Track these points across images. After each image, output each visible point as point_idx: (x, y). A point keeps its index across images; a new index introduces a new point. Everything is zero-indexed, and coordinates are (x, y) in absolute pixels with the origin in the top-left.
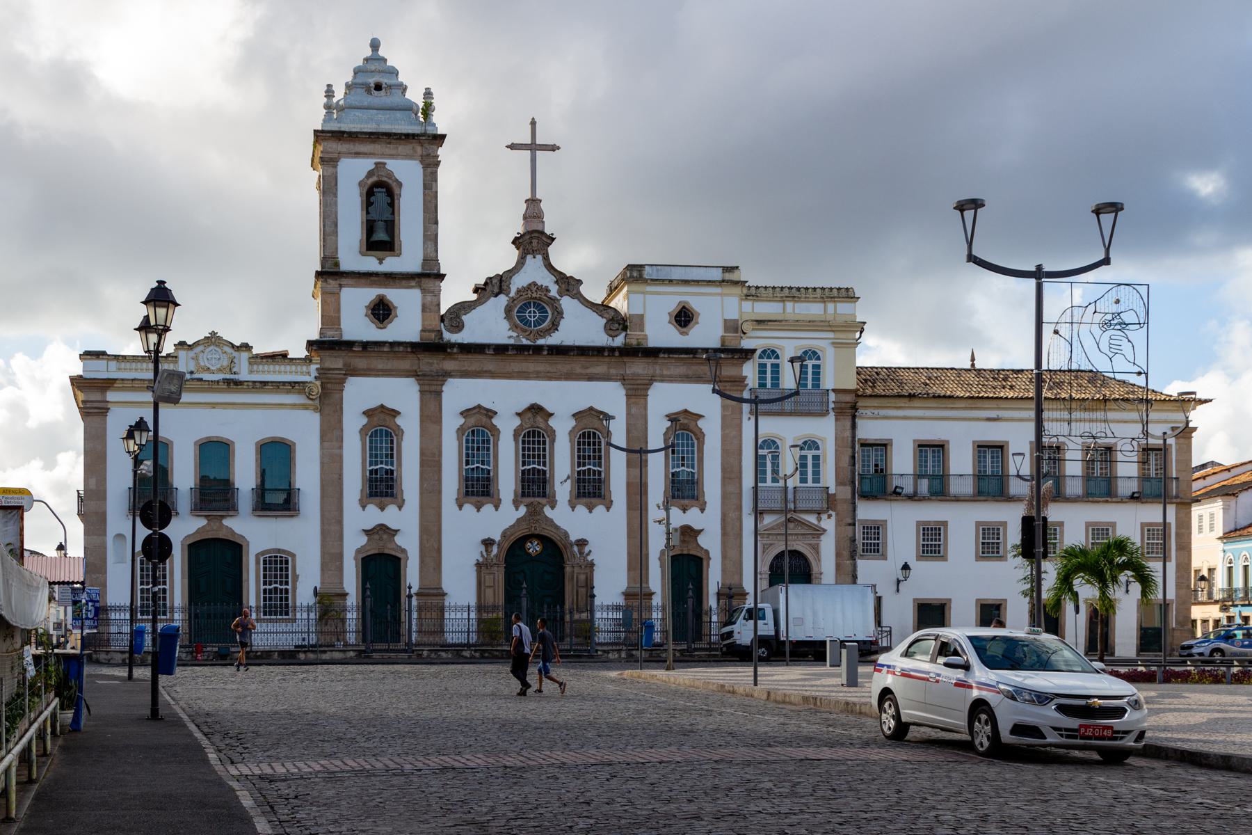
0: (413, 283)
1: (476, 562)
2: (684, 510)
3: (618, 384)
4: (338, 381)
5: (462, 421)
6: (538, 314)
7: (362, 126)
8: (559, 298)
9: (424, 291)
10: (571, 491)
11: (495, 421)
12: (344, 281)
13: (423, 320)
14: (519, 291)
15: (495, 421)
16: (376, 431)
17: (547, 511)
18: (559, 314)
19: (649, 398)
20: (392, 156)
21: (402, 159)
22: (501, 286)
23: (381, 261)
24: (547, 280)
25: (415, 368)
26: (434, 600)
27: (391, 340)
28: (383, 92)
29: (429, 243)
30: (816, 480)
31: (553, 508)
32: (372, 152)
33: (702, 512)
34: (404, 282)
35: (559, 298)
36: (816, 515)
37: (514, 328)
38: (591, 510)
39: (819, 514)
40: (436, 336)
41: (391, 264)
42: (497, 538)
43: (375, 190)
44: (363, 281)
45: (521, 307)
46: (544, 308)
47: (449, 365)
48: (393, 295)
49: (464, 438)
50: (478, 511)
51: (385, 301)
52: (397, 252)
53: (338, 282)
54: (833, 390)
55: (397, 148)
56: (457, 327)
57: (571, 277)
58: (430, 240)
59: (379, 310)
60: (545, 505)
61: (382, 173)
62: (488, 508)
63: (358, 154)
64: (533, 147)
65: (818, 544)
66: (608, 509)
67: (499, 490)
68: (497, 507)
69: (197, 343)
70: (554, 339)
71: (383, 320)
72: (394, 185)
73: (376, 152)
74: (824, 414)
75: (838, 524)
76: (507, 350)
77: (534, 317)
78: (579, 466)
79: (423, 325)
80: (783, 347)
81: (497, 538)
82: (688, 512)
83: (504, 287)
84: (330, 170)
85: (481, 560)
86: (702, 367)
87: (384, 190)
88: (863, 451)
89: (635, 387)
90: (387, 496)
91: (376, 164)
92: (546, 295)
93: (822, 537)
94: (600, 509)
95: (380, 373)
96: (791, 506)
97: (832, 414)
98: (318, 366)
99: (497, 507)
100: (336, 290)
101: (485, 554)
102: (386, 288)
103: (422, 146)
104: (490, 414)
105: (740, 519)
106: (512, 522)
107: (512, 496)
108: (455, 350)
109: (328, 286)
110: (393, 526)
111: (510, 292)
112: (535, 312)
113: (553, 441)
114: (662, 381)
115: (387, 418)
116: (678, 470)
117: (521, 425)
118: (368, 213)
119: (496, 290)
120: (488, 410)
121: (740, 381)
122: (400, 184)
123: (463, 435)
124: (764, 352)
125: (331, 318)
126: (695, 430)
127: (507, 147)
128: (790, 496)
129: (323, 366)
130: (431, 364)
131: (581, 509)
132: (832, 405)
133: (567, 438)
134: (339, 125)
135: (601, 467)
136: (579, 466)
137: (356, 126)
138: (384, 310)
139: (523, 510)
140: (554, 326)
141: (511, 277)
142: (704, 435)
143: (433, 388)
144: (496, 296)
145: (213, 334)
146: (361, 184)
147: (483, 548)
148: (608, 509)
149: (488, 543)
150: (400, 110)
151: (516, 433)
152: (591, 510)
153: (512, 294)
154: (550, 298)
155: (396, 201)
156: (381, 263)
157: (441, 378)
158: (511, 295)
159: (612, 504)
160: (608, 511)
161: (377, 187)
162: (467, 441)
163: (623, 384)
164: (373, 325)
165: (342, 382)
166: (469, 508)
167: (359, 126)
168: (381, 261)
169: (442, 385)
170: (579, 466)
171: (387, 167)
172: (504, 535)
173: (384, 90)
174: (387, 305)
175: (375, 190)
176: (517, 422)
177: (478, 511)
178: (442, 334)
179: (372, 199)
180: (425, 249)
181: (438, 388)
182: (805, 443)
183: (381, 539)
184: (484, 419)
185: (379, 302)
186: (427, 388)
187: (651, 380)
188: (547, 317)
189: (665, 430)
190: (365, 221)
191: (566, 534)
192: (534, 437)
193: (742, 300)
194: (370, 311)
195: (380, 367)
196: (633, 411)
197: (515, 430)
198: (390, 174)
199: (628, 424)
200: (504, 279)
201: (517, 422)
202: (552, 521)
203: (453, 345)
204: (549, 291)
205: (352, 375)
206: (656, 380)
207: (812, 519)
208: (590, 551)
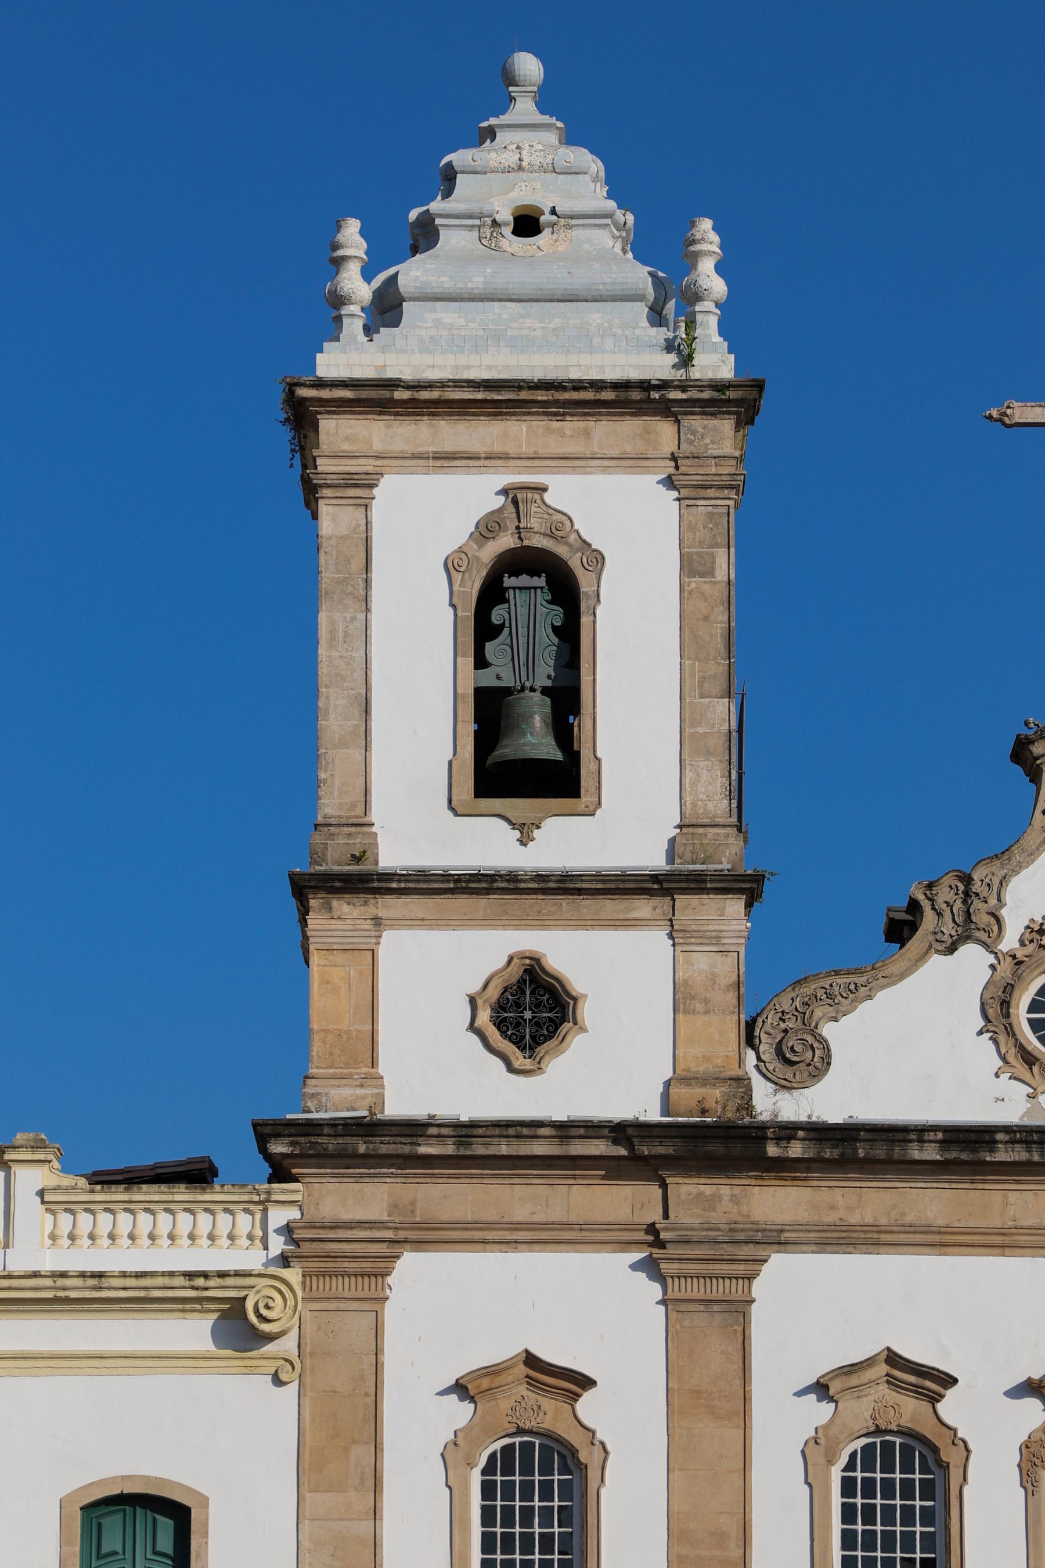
4: (367, 1265)
7: (463, 360)
12: (388, 906)
16: (508, 1450)
20: (568, 461)
21: (605, 470)
22: (968, 914)
23: (525, 832)
25: (655, 1215)
27: (560, 1115)
28: (543, 239)
29: (703, 764)
32: (497, 448)
37: (1022, 1069)
43: (508, 581)
44: (462, 902)
49: (836, 1474)
52: (587, 798)
53: (371, 910)
55: (587, 433)
58: (708, 754)
59: (518, 1005)
61: (534, 523)
71: (537, 1041)
72: (574, 562)
73: (512, 451)
76: (991, 1145)
83: (981, 918)
87: (541, 581)
100: (361, 942)
102: (545, 927)
109: (336, 924)
115: (548, 1404)
118: (481, 662)
119: (949, 928)
122: (599, 559)
123: (830, 1462)
129: (312, 1215)
130: (712, 1203)
134: (379, 359)
137: (439, 360)
141: (1003, 882)
143: (719, 1290)
144: (951, 950)
150: (599, 299)
153: (1009, 942)
155: (585, 620)
157: (745, 1251)
161: (515, 573)
162: (848, 1487)
167: (450, 360)
168: (525, 832)
169: (750, 1278)
173: (546, 233)
174: (552, 991)
175: (508, 581)
178: (749, 1090)
179: (498, 614)
181: (734, 1290)
185: (521, 982)
186: (695, 1290)
194: (484, 1017)
195: (521, 1214)
197: (1026, 1446)
200: (976, 887)
203: (788, 1131)
205: (419, 1245)
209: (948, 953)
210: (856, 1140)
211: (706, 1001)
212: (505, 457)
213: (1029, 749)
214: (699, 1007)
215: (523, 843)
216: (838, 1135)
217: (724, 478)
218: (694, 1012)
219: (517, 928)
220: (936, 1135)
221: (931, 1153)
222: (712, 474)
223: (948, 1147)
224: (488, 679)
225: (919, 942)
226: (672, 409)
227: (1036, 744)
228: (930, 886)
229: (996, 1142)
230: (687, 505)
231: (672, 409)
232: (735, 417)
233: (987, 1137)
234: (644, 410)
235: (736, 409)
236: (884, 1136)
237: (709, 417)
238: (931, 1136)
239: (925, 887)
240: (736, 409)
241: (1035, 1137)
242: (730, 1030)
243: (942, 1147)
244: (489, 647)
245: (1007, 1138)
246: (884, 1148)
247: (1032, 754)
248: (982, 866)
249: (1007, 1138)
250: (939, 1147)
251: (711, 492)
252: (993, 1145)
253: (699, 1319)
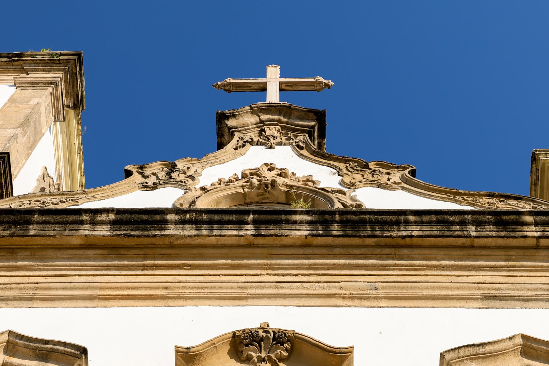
209: (150, 189)
210: (29, 222)
213: (224, 122)
216: (12, 218)
217: (48, 79)
220: (108, 216)
221: (103, 231)
222: (40, 78)
223: (120, 228)
225: (126, 186)
226: (25, 67)
227: (230, 120)
228: (142, 167)
229: (165, 222)
230: (21, 89)
231: (25, 67)
232: (63, 72)
233: (158, 217)
234: (8, 70)
235: (63, 67)
236: (57, 218)
237: (47, 73)
238: (103, 217)
239: (138, 168)
240: (63, 67)
241: (205, 217)
243: (114, 227)
245: (177, 217)
246: (56, 229)
247: (227, 125)
248: (185, 162)
249: (177, 217)
250: (111, 228)
252: (163, 226)
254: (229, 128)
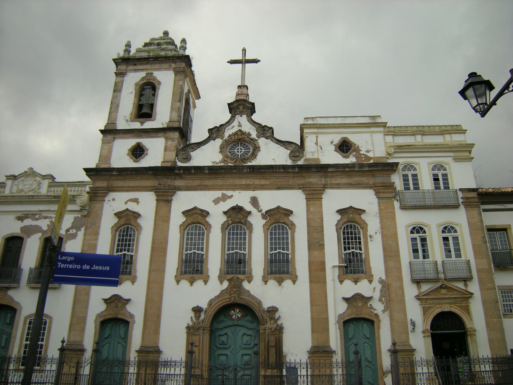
0: (160, 134)
1: (186, 325)
2: (356, 282)
3: (300, 191)
5: (184, 219)
6: (243, 150)
8: (257, 139)
9: (167, 139)
10: (264, 269)
11: (208, 219)
12: (117, 136)
13: (165, 155)
14: (230, 136)
15: (208, 219)
17: (246, 285)
18: (257, 149)
19: (324, 201)
20: (157, 70)
21: (163, 71)
23: (142, 124)
24: (247, 128)
26: (151, 357)
30: (458, 255)
31: (249, 282)
33: (371, 283)
34: (153, 134)
35: (257, 139)
36: (463, 283)
38: (280, 282)
39: (465, 281)
40: (171, 164)
41: (149, 125)
42: (204, 305)
43: (145, 87)
45: (232, 147)
46: (247, 146)
47: (178, 183)
48: (146, 142)
50: (191, 285)
51: (141, 146)
52: (153, 118)
54: (461, 190)
56: (186, 158)
57: (266, 126)
59: (137, 151)
60: (243, 280)
62: (199, 283)
63: (136, 70)
64: (244, 62)
65: (468, 306)
66: (294, 282)
67: (208, 269)
68: (206, 282)
69: (21, 175)
70: (254, 163)
71: (139, 157)
72: (156, 84)
74: (456, 207)
75: (481, 289)
77: (241, 152)
78: (271, 250)
79: (164, 159)
80: (419, 163)
81: (204, 305)
82: (359, 284)
84: (119, 79)
85: (191, 324)
86: (362, 178)
87: (150, 87)
88: (490, 234)
89: (312, 192)
90: (126, 274)
91: (147, 74)
92: (248, 137)
93: (470, 300)
94: (288, 283)
95: (131, 189)
96: (442, 276)
97: (462, 207)
98: (91, 186)
99: (206, 282)
101: (194, 319)
103: (175, 63)
104: (204, 213)
105: (401, 288)
106: (218, 293)
107: (218, 273)
108: (181, 172)
110: (126, 297)
111: (224, 137)
112: (241, 149)
113: (251, 232)
114: (332, 188)
116: (349, 252)
117: (228, 221)
118: (140, 100)
120: (202, 211)
121: (391, 186)
124: (405, 167)
125: (105, 156)
126: (359, 221)
127: (228, 62)
128: (440, 268)
131: (272, 283)
132: (461, 201)
133: (262, 230)
135: (288, 251)
136: (271, 250)
138: (140, 151)
139: (226, 284)
140: (254, 155)
142: (367, 225)
143: (165, 198)
145: (31, 169)
146: (136, 84)
147: (192, 314)
148: (294, 282)
149: (197, 310)
151: (224, 227)
152: (280, 282)
154: (250, 139)
156: (142, 125)
158: (224, 139)
159: (297, 279)
160: (294, 284)
161: (146, 86)
163: (303, 191)
164: (132, 161)
165: (106, 195)
166: (184, 283)
168: (142, 124)
169: (173, 195)
170: (271, 250)
171: (154, 75)
172: (210, 303)
176: (224, 219)
177: (191, 285)
179: (143, 93)
180: (171, 116)
181: (169, 198)
182: (445, 228)
183: (117, 307)
184: (200, 217)
187: (325, 187)
188: (250, 151)
189: (336, 222)
190: (137, 104)
191: (260, 303)
192: (237, 230)
193: (385, 135)
196: (312, 209)
198: (155, 79)
199: (308, 219)
201: (224, 219)
202: (248, 292)
204: (251, 135)
206: (327, 188)
207: (460, 285)
208: (280, 316)
211: (170, 149)
212: (147, 69)
214: (168, 150)
215: (142, 125)
218: (167, 151)
219: (138, 138)
224: (141, 103)
242: (174, 154)
244: (142, 98)
251: (180, 73)
253: (161, 203)
254: (231, 108)
